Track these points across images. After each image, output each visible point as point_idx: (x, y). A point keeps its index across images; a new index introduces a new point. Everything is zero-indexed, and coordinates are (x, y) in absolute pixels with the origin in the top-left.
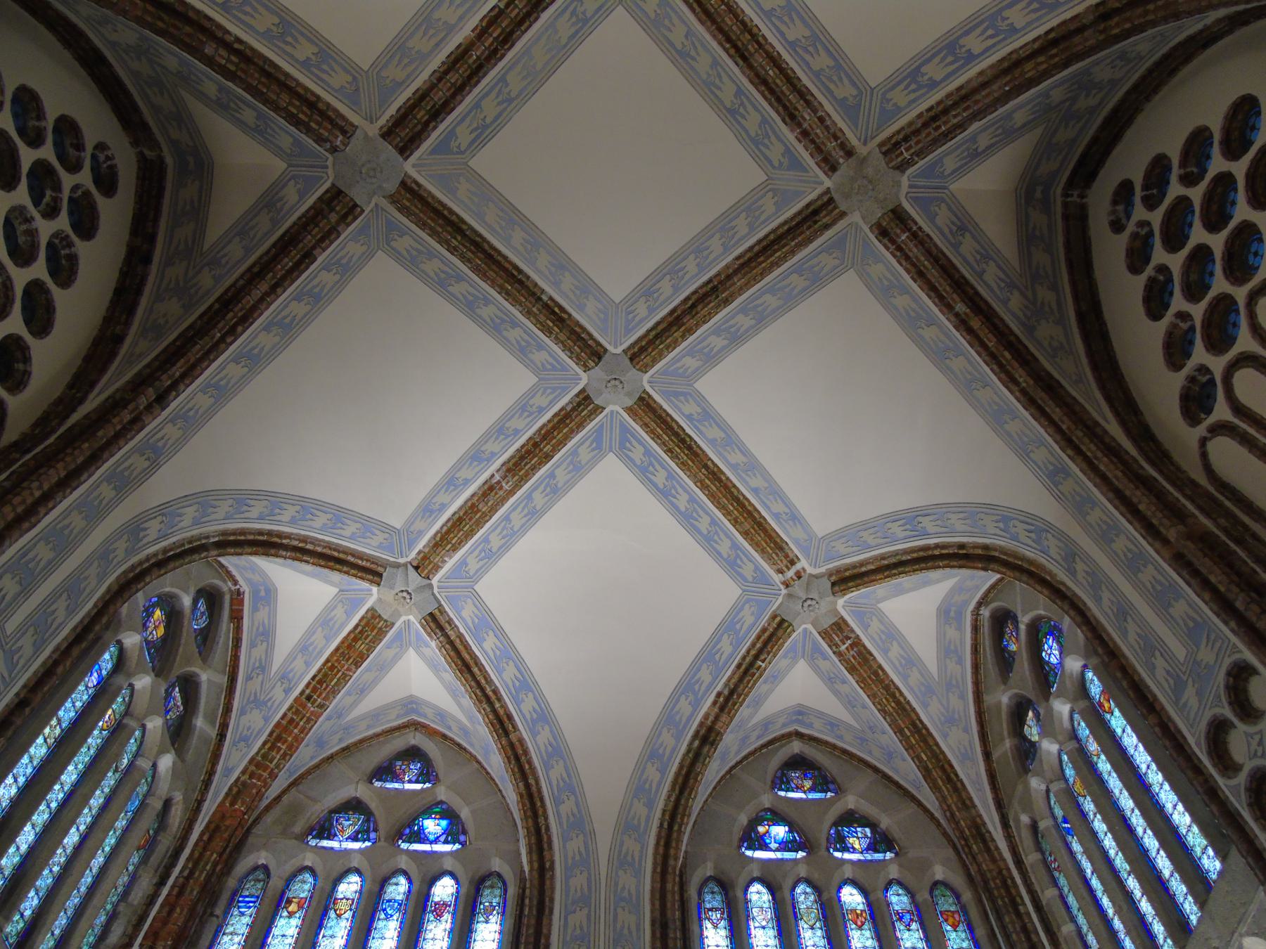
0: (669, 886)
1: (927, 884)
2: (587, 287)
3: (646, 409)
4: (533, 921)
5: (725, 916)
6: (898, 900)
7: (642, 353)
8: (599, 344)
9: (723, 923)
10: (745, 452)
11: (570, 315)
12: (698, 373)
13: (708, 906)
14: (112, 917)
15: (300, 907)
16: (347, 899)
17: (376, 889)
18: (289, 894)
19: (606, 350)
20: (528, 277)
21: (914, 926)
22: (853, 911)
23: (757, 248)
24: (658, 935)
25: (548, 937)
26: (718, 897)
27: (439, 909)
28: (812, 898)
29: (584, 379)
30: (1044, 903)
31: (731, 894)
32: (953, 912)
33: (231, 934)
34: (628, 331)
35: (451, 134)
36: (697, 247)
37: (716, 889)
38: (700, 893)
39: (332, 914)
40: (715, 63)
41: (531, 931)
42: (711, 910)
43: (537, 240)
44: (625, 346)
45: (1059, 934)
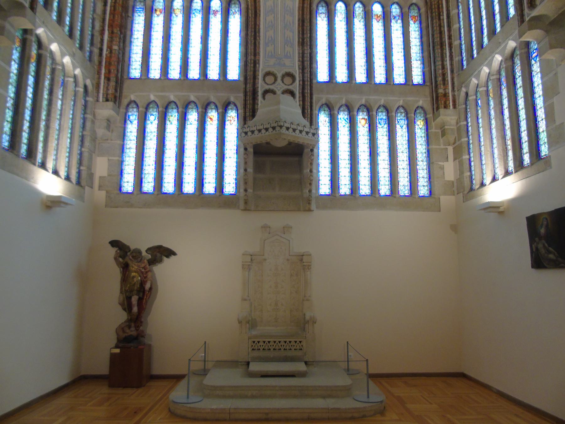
0: (305, 5)
1: (409, 4)
4: (253, 20)
5: (327, 16)
6: (395, 10)
9: (326, 19)
13: (320, 12)
14: (93, 20)
15: (161, 13)
16: (179, 9)
17: (189, 5)
18: (155, 7)
21: (400, 21)
22: (377, 15)
24: (301, 25)
25: (259, 26)
26: (324, 8)
27: (215, 12)
28: (361, 9)
30: (451, 15)
31: (330, 7)
32: (416, 16)
33: (138, 23)
37: (324, 5)
38: (317, 6)
39: (174, 15)
41: (253, 23)
42: (321, 13)
45: (452, 28)
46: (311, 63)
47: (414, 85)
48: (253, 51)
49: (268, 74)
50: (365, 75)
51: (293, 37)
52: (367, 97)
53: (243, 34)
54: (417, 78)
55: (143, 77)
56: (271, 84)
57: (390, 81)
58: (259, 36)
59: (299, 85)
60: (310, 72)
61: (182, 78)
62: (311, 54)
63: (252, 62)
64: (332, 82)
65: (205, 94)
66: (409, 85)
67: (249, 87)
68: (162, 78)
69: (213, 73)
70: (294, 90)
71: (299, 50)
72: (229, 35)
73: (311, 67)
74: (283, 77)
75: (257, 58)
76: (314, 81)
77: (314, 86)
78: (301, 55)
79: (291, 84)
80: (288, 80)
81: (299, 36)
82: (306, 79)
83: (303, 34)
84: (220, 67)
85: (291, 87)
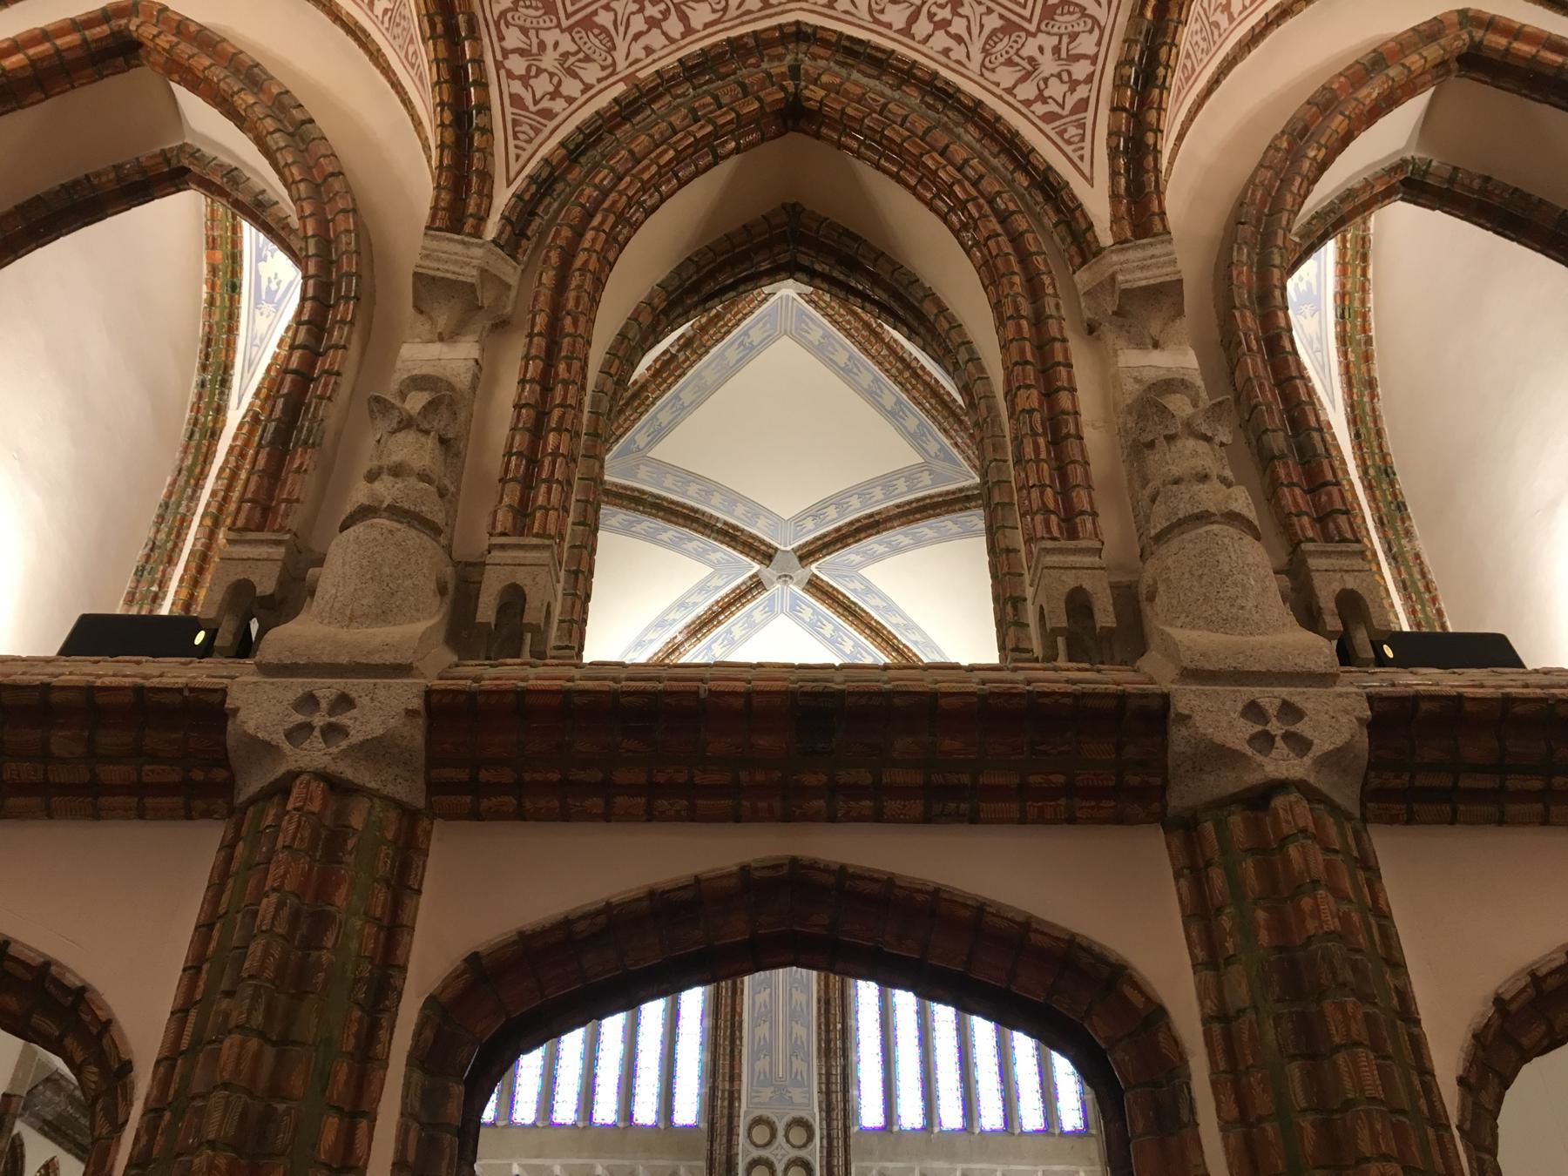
2: (756, 510)
3: (816, 587)
4: (729, 1001)
7: (808, 554)
8: (769, 546)
10: (904, 617)
11: (742, 531)
12: (862, 565)
19: (776, 549)
20: (704, 514)
23: (914, 505)
29: (756, 567)
34: (796, 538)
35: (633, 441)
36: (862, 490)
40: (876, 380)
41: (729, 1009)
43: (709, 487)
44: (795, 545)
46: (845, 1091)
47: (1063, 1134)
48: (727, 1070)
49: (758, 1121)
50: (960, 1112)
51: (808, 1035)
52: (965, 1166)
53: (708, 1022)
54: (1071, 1115)
55: (500, 1123)
56: (765, 1146)
57: (1012, 1127)
58: (741, 1039)
59: (821, 1147)
60: (845, 1109)
61: (580, 1124)
62: (845, 1068)
63: (726, 1095)
64: (891, 1132)
65: (627, 1162)
66: (1053, 1134)
67: (720, 1150)
68: (539, 1124)
69: (646, 1112)
70: (810, 1158)
71: (820, 1068)
72: (681, 1023)
73: (846, 1100)
74: (789, 1126)
75: (736, 1087)
76: (855, 1129)
77: (852, 1142)
78: (823, 1077)
79: (804, 1146)
80: (798, 1135)
81: (819, 1034)
82: (834, 1133)
83: (828, 1031)
84: (659, 1096)
85: (802, 1153)
